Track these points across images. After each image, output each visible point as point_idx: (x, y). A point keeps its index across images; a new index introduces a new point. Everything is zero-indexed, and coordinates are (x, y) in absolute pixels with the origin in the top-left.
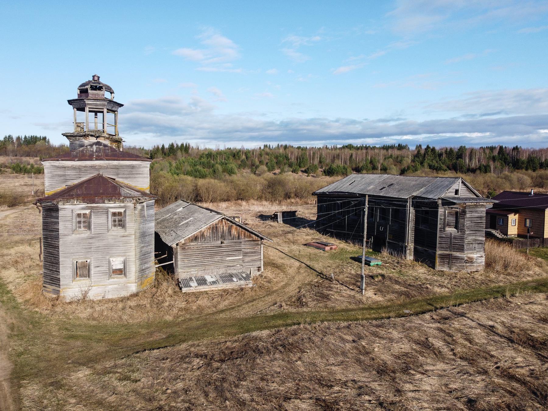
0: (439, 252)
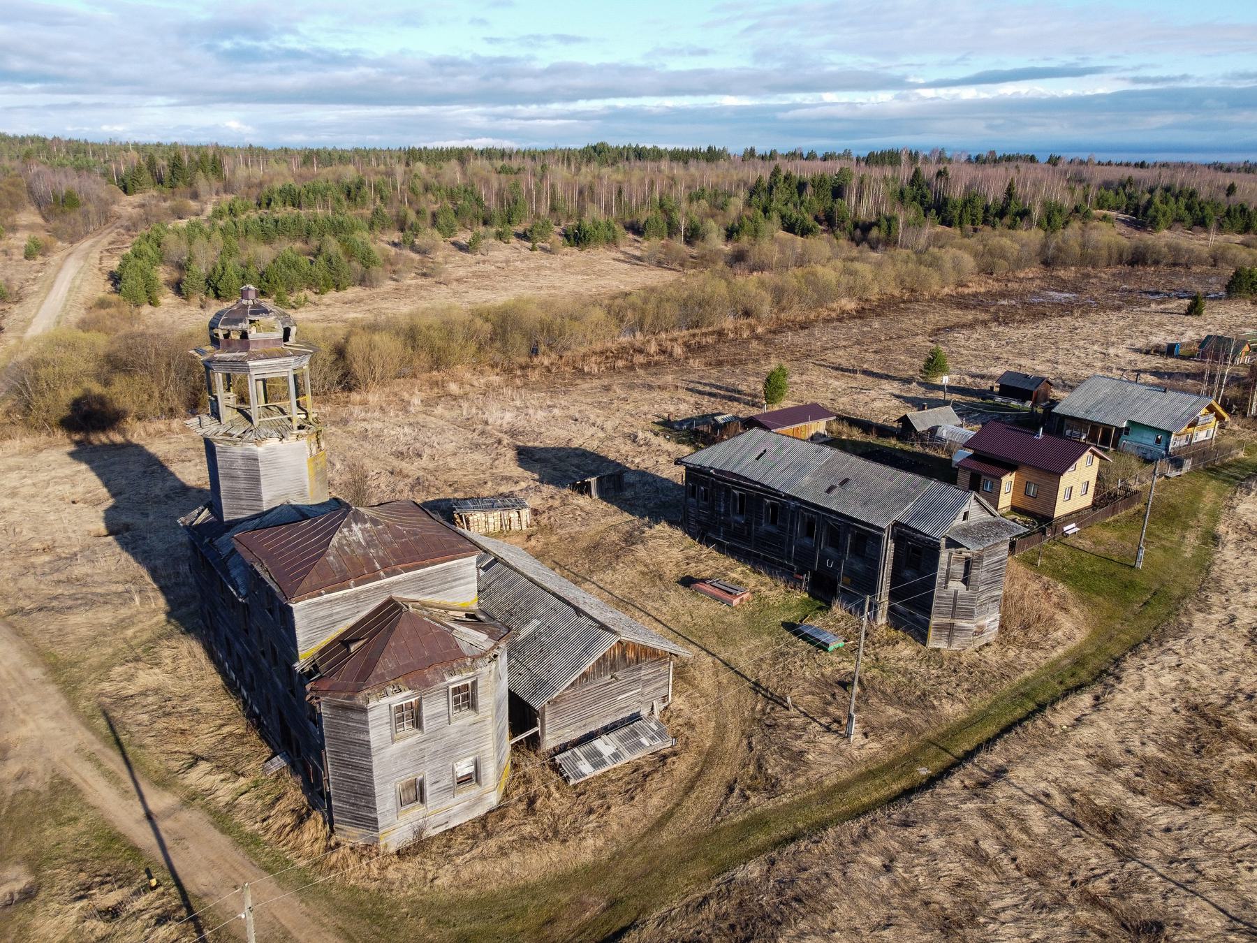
0: (934, 620)
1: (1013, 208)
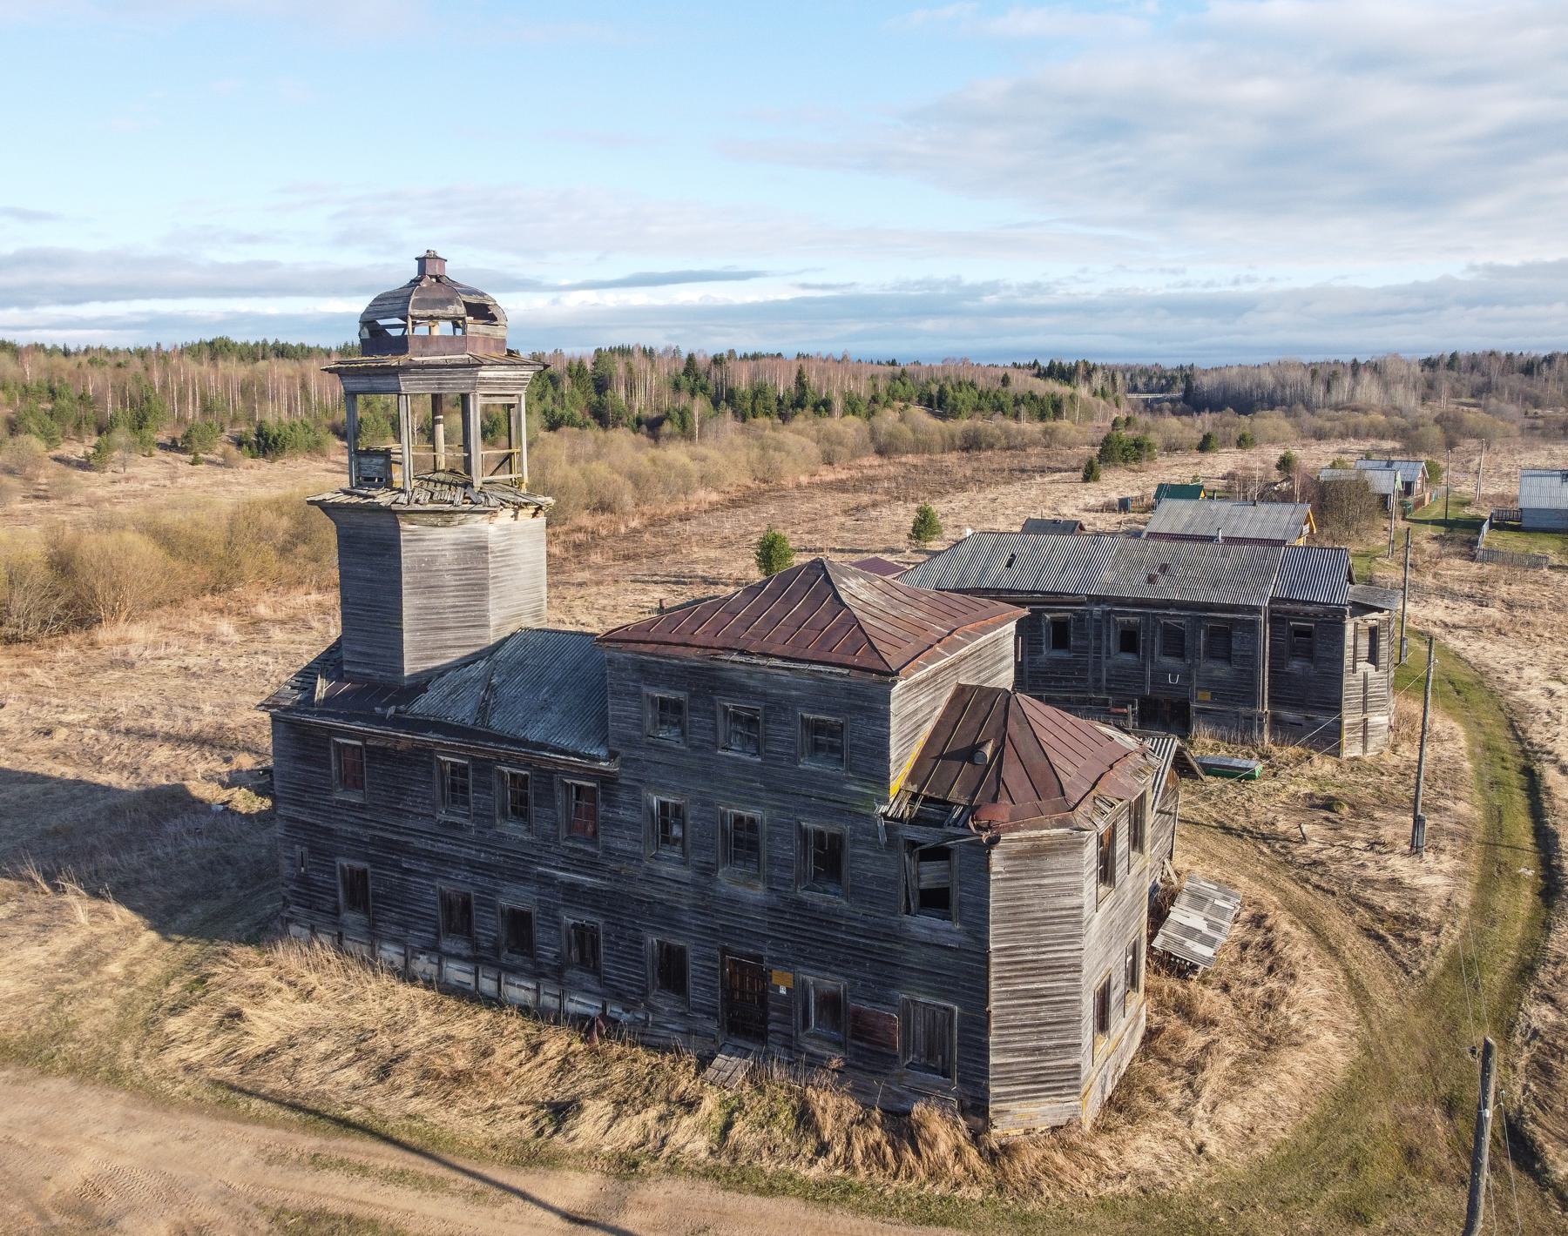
1: (810, 398)
